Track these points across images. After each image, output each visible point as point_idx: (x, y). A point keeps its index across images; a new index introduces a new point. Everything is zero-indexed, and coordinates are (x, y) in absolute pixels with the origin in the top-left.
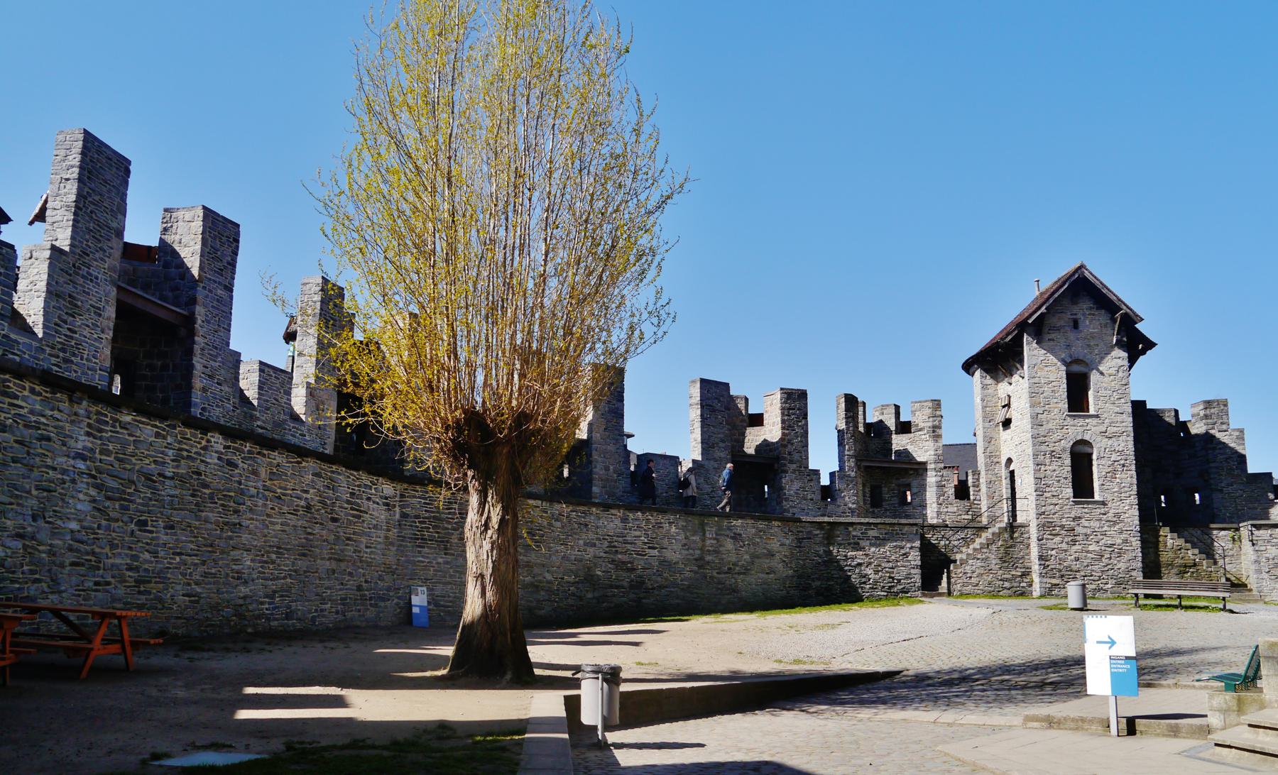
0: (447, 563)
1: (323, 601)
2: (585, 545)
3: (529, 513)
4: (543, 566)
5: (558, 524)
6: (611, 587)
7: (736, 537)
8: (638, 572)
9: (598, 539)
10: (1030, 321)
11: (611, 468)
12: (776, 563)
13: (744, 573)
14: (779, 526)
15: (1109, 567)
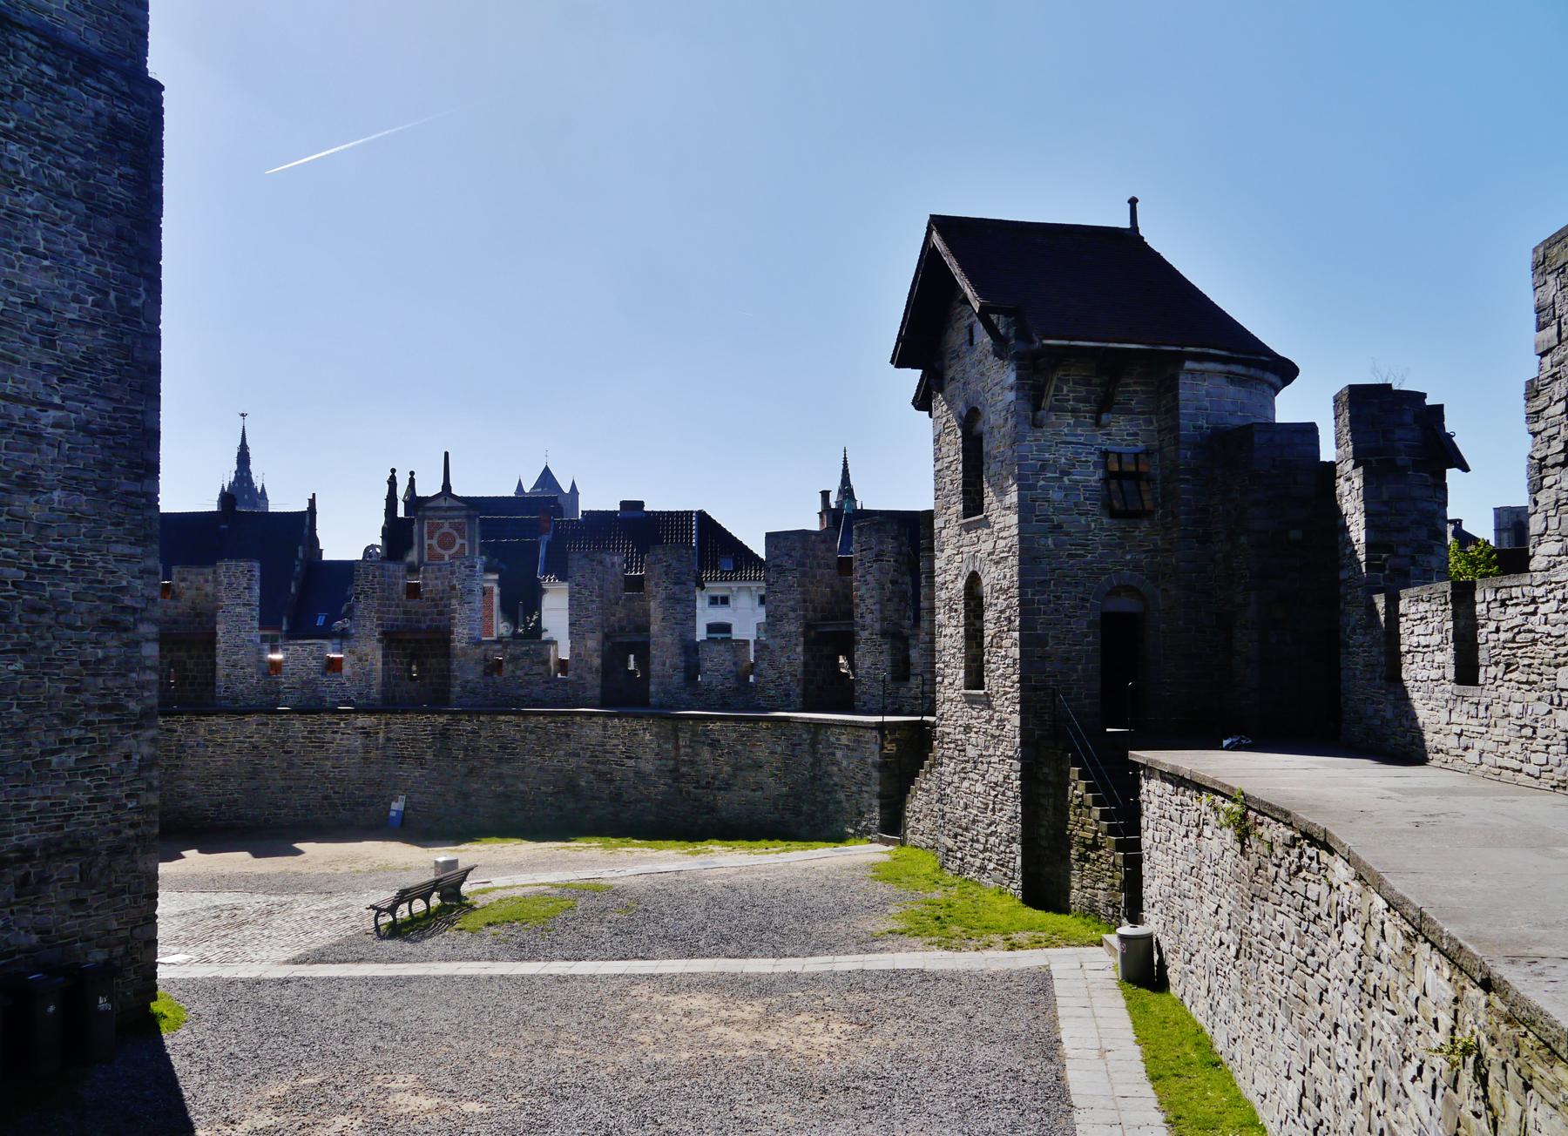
0: (422, 776)
1: (278, 808)
2: (565, 755)
3: (500, 729)
4: (517, 776)
5: (534, 737)
6: (594, 798)
7: (714, 744)
8: (617, 783)
9: (582, 749)
10: (401, 513)
11: (668, 661)
12: (764, 776)
13: (725, 789)
14: (768, 729)
15: (993, 828)
